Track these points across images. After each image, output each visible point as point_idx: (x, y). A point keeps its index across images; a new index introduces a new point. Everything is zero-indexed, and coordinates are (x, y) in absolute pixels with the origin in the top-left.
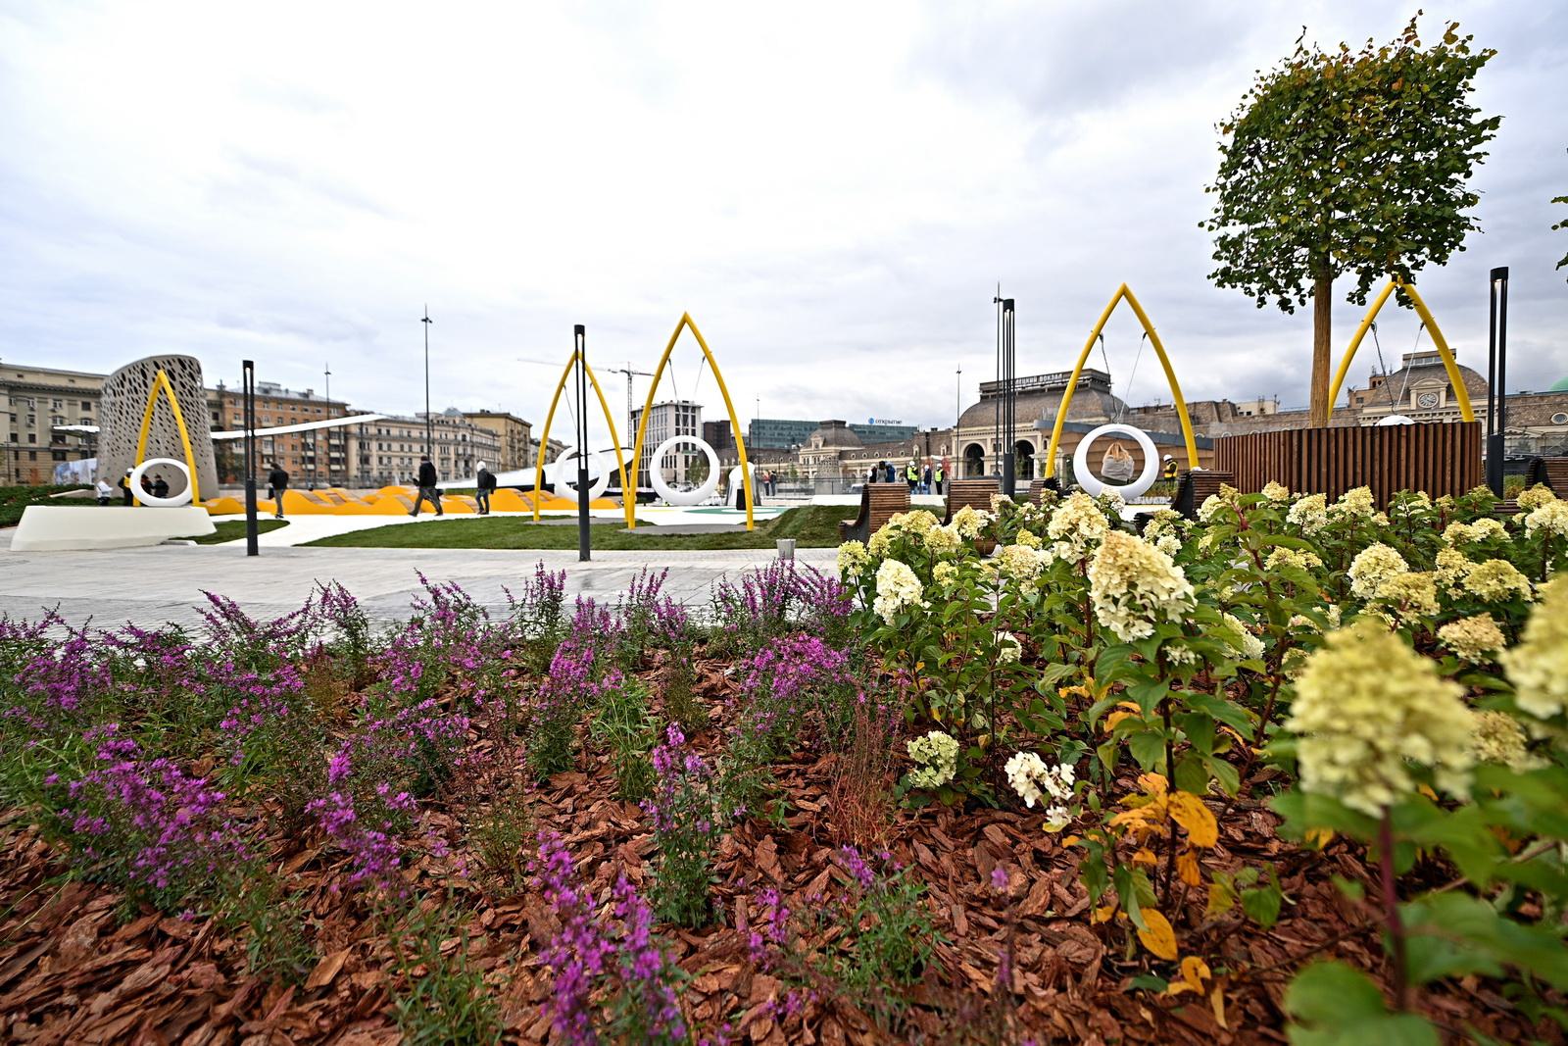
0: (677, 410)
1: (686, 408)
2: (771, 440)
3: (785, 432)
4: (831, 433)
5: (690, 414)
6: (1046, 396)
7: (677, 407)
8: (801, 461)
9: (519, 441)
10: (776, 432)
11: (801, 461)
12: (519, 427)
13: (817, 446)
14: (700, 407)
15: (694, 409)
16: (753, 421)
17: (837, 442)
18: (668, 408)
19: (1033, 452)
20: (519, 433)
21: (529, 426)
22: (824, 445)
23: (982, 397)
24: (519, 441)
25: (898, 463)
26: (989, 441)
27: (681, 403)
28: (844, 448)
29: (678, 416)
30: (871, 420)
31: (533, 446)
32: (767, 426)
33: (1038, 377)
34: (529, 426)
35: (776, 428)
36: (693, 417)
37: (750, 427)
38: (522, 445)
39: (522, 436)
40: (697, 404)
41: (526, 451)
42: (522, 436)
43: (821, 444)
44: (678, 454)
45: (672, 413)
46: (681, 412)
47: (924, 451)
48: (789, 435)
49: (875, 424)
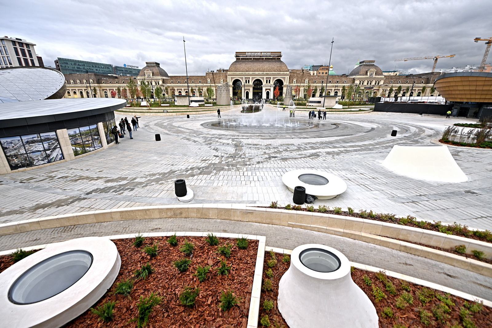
1: (21, 44)
2: (73, 71)
3: (81, 67)
4: (156, 70)
5: (25, 48)
7: (14, 42)
10: (76, 67)
14: (33, 45)
15: (28, 45)
22: (153, 75)
25: (196, 86)
28: (164, 78)
33: (261, 52)
35: (75, 64)
43: (151, 75)
46: (18, 46)
47: (213, 81)
48: (84, 69)
49: (127, 67)
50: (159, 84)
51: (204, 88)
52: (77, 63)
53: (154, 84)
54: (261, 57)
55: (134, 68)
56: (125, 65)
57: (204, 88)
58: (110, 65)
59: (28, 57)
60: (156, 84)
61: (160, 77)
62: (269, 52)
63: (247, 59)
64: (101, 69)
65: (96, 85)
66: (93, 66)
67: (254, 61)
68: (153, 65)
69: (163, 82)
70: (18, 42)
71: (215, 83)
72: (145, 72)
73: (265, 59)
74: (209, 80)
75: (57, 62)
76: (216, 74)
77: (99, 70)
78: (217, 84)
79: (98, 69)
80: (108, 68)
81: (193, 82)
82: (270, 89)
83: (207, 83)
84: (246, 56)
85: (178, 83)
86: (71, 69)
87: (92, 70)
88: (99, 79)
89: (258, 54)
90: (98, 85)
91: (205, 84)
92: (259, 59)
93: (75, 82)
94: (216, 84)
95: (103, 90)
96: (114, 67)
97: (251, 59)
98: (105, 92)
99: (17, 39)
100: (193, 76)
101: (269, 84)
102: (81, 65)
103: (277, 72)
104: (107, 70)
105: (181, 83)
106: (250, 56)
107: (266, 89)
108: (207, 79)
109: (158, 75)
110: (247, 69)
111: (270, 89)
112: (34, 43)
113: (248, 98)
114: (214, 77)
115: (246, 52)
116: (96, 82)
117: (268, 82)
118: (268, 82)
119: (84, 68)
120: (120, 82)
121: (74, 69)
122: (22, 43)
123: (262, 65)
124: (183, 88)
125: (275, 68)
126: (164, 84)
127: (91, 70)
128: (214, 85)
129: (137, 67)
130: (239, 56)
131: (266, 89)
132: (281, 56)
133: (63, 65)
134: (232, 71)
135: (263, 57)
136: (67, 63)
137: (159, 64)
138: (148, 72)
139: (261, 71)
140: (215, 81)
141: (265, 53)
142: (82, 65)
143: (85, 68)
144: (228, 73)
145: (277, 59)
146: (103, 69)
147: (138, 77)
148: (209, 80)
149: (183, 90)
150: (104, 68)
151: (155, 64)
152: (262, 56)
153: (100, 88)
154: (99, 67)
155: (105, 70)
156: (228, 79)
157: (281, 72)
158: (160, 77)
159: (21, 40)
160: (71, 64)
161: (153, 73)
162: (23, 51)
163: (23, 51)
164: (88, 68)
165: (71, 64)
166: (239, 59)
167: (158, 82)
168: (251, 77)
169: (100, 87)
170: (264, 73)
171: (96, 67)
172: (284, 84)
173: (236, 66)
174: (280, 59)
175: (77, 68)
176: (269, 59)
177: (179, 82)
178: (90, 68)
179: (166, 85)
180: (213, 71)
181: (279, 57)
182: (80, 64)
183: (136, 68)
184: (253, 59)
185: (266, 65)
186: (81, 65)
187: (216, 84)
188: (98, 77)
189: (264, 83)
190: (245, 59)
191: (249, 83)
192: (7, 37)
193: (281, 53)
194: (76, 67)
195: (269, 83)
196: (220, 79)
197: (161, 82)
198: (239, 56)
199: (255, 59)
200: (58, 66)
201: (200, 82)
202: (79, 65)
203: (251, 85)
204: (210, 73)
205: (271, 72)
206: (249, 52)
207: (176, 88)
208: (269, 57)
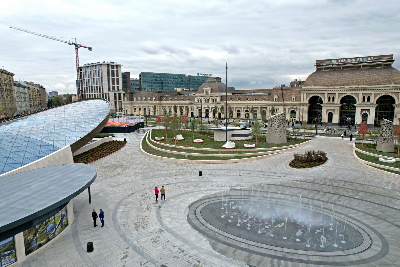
0: (108, 67)
1: (113, 66)
2: (151, 83)
3: (158, 79)
5: (115, 69)
6: (362, 70)
7: (108, 66)
8: (196, 101)
9: (6, 85)
10: (154, 79)
11: (196, 101)
12: (5, 76)
13: (207, 92)
14: (121, 66)
15: (117, 66)
16: (143, 73)
17: (220, 90)
18: (103, 66)
19: (355, 103)
20: (5, 80)
21: (12, 75)
22: (211, 92)
23: (318, 69)
24: (6, 85)
26: (326, 95)
27: (109, 63)
29: (108, 71)
30: (198, 74)
31: (15, 87)
32: (149, 76)
33: (356, 58)
34: (12, 75)
35: (154, 77)
36: (117, 72)
37: (140, 76)
38: (8, 87)
39: (7, 81)
40: (118, 63)
41: (11, 91)
42: (7, 81)
43: (210, 91)
44: (110, 93)
45: (105, 69)
47: (281, 98)
48: (160, 80)
49: (200, 75)
50: (216, 101)
51: (268, 107)
52: (156, 76)
53: (211, 101)
54: (357, 65)
55: (206, 76)
56: (198, 74)
57: (268, 107)
58: (184, 75)
59: (115, 77)
60: (213, 102)
61: (218, 94)
62: (370, 57)
63: (334, 68)
64: (175, 80)
65: (157, 102)
66: (168, 78)
67: (343, 70)
68: (213, 80)
69: (222, 100)
70: (111, 65)
71: (283, 101)
72: (204, 88)
73: (363, 66)
74: (276, 97)
75: (141, 76)
76: (287, 88)
77: (173, 80)
78: (287, 102)
79: (173, 80)
80: (182, 78)
81: (256, 99)
82: (369, 111)
83: (273, 101)
84: (332, 65)
85: (237, 101)
86: (150, 81)
87: (167, 81)
88: (161, 97)
89: (351, 60)
90: (159, 102)
91: (270, 102)
92: (353, 67)
93: (142, 100)
94: (285, 102)
95: (163, 107)
96: (187, 76)
97: (339, 68)
98: (164, 109)
99: (111, 62)
100: (260, 90)
101: (368, 103)
102: (158, 77)
103: (382, 84)
104: (180, 80)
105: (241, 101)
106: (339, 64)
107: (362, 110)
108: (273, 96)
109: (216, 92)
110: (332, 83)
111: (369, 111)
112: (122, 65)
113: (331, 122)
114: (284, 92)
115: (331, 60)
116: (158, 99)
117: (366, 100)
118: (366, 100)
119: (161, 79)
120: (179, 99)
121: (152, 81)
122: (114, 66)
123: (357, 75)
124: (243, 107)
125: (380, 78)
126: (221, 102)
127: (166, 82)
128: (282, 103)
129: (210, 75)
130: (321, 66)
131: (362, 110)
132: (392, 61)
133: (144, 79)
134: (309, 85)
135: (359, 65)
136: (147, 77)
137: (220, 79)
138: (207, 88)
139: (354, 85)
140: (284, 98)
141: (364, 59)
142: (159, 77)
143: (162, 79)
144: (303, 87)
145: (385, 65)
146: (176, 80)
147: (196, 94)
148: (276, 97)
149: (242, 108)
150: (177, 78)
151: (216, 80)
152: (358, 63)
153: (160, 105)
154: (173, 78)
155: (178, 80)
156: (302, 95)
157: (391, 84)
158: (218, 94)
159: (113, 63)
160: (151, 77)
161: (212, 90)
162: (113, 72)
163: (113, 72)
164: (164, 79)
165: (151, 77)
166: (321, 69)
167: (216, 99)
168: (337, 93)
169: (161, 104)
170: (360, 87)
171: (171, 78)
172: (397, 103)
173: (315, 78)
174: (390, 65)
175: (155, 80)
176: (370, 66)
177: (239, 99)
178: (165, 80)
179: (223, 103)
180: (285, 85)
181: (389, 63)
182: (158, 76)
183: (209, 76)
184: (343, 67)
185: (364, 75)
186: (158, 77)
187: (285, 102)
188: (161, 95)
189: (359, 100)
190: (330, 68)
191: (333, 100)
192: (105, 62)
193: (393, 56)
194: (154, 79)
195: (368, 100)
196: (291, 95)
197: (218, 100)
198: (321, 66)
199: (346, 67)
200: (141, 79)
201: (264, 99)
202: (157, 77)
203: (337, 104)
204: (278, 88)
205: (373, 84)
206: (336, 59)
207: (235, 107)
208: (371, 64)
